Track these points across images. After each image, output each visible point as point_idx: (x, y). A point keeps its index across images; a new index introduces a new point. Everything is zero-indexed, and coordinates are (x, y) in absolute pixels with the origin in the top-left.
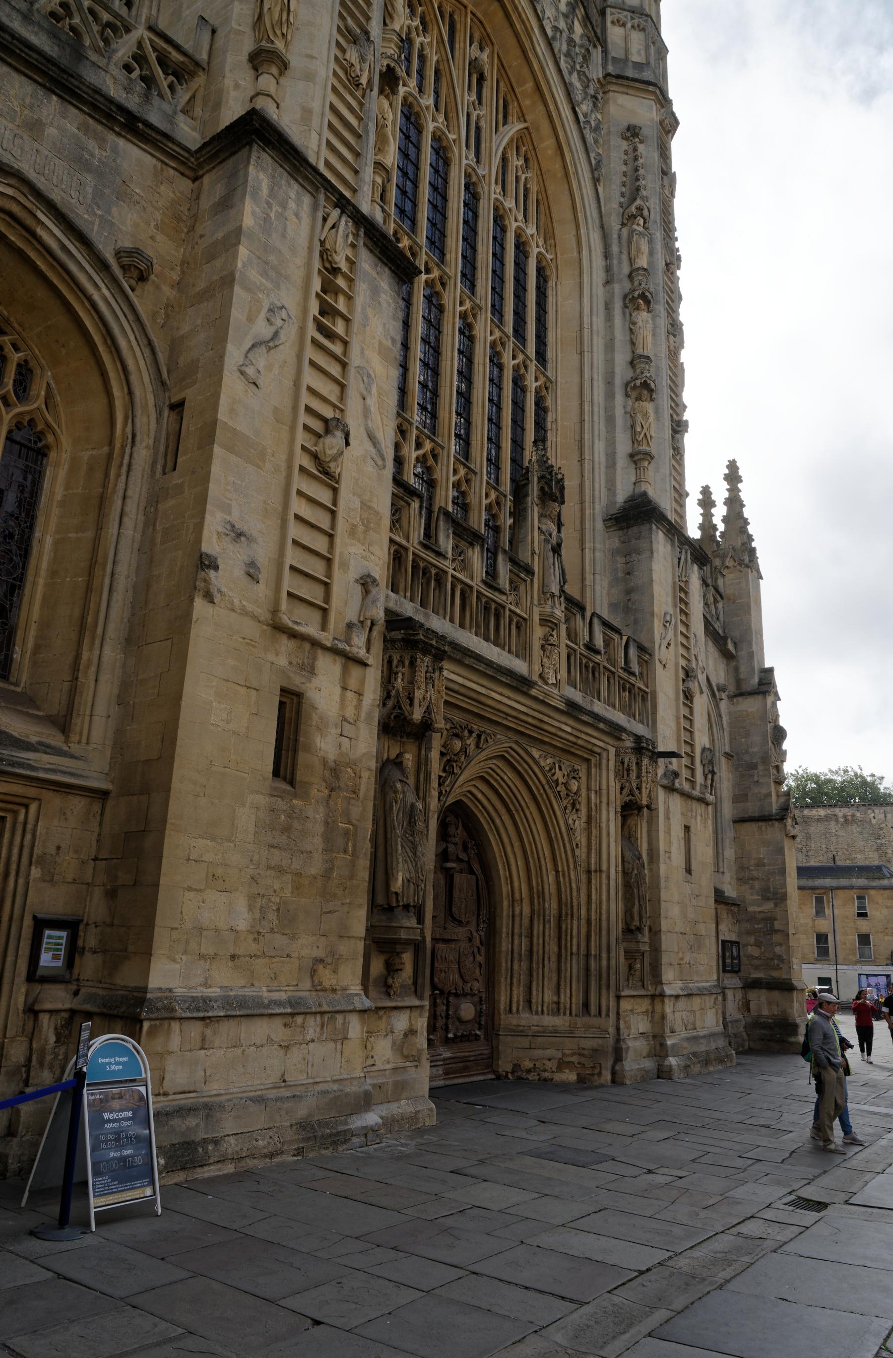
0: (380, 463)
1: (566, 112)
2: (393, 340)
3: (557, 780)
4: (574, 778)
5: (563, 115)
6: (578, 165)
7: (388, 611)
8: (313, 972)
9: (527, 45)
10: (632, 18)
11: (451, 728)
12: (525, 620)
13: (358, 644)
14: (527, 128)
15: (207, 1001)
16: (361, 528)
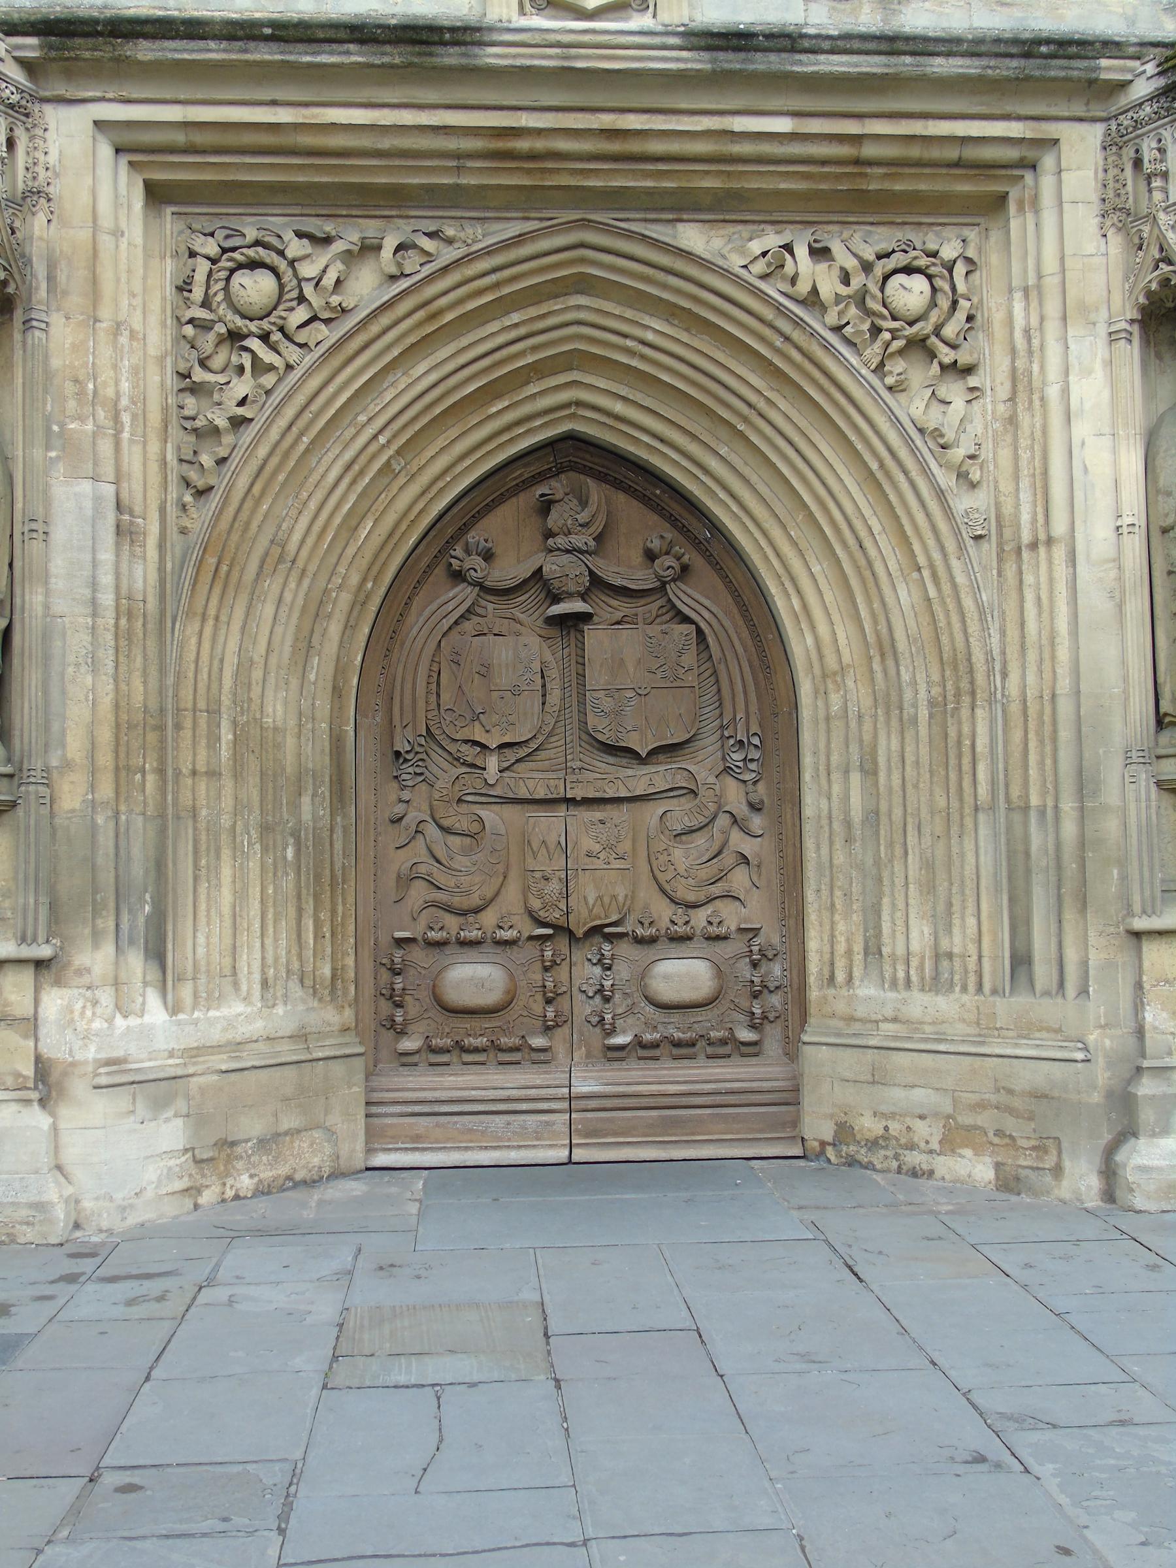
3: (815, 291)
4: (908, 270)
11: (225, 251)
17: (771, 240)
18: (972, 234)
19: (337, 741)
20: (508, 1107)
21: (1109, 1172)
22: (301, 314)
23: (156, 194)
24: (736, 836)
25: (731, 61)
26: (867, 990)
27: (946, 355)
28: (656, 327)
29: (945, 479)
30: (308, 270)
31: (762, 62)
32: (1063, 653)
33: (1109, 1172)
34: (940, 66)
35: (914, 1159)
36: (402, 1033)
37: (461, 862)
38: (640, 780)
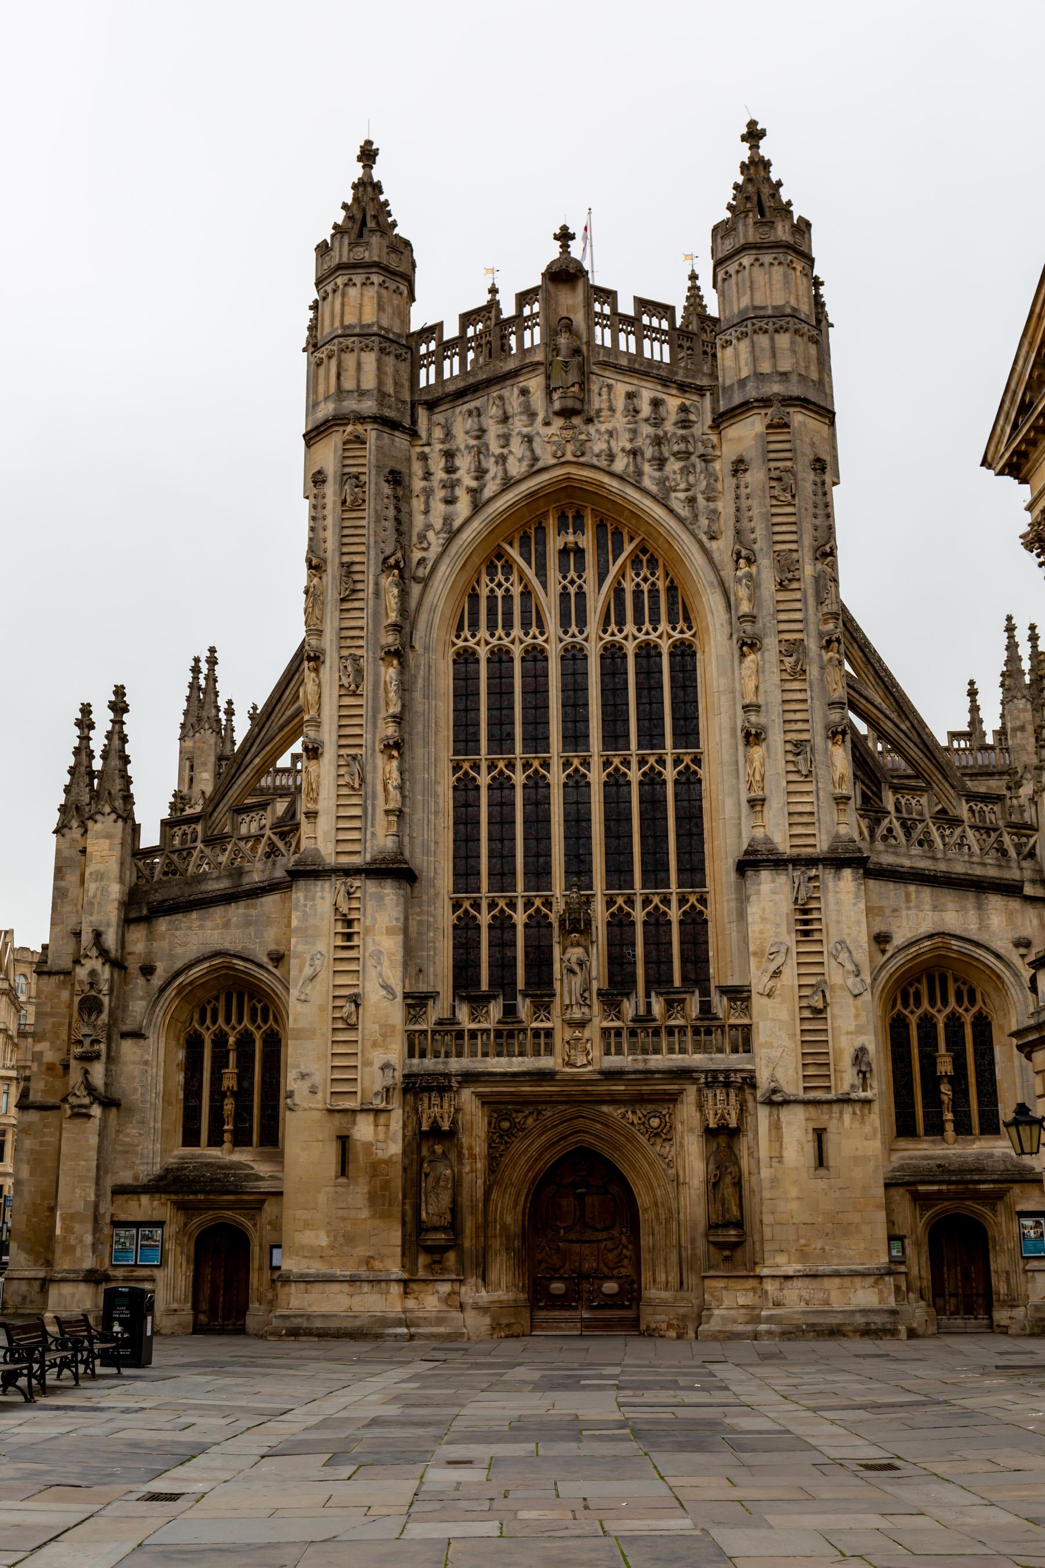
0: (391, 997)
1: (658, 512)
2: (397, 919)
4: (655, 1117)
7: (404, 1076)
12: (553, 1029)
13: (379, 1103)
14: (643, 539)
15: (307, 1275)
16: (380, 1038)
17: (623, 1110)
19: (523, 1226)
20: (566, 1320)
21: (696, 1333)
23: (483, 1103)
24: (624, 1251)
26: (653, 1291)
27: (664, 1137)
28: (599, 1126)
29: (665, 1166)
30: (517, 1120)
31: (616, 1077)
33: (696, 1333)
34: (657, 1076)
35: (662, 1333)
36: (540, 1301)
37: (554, 1257)
38: (600, 1236)
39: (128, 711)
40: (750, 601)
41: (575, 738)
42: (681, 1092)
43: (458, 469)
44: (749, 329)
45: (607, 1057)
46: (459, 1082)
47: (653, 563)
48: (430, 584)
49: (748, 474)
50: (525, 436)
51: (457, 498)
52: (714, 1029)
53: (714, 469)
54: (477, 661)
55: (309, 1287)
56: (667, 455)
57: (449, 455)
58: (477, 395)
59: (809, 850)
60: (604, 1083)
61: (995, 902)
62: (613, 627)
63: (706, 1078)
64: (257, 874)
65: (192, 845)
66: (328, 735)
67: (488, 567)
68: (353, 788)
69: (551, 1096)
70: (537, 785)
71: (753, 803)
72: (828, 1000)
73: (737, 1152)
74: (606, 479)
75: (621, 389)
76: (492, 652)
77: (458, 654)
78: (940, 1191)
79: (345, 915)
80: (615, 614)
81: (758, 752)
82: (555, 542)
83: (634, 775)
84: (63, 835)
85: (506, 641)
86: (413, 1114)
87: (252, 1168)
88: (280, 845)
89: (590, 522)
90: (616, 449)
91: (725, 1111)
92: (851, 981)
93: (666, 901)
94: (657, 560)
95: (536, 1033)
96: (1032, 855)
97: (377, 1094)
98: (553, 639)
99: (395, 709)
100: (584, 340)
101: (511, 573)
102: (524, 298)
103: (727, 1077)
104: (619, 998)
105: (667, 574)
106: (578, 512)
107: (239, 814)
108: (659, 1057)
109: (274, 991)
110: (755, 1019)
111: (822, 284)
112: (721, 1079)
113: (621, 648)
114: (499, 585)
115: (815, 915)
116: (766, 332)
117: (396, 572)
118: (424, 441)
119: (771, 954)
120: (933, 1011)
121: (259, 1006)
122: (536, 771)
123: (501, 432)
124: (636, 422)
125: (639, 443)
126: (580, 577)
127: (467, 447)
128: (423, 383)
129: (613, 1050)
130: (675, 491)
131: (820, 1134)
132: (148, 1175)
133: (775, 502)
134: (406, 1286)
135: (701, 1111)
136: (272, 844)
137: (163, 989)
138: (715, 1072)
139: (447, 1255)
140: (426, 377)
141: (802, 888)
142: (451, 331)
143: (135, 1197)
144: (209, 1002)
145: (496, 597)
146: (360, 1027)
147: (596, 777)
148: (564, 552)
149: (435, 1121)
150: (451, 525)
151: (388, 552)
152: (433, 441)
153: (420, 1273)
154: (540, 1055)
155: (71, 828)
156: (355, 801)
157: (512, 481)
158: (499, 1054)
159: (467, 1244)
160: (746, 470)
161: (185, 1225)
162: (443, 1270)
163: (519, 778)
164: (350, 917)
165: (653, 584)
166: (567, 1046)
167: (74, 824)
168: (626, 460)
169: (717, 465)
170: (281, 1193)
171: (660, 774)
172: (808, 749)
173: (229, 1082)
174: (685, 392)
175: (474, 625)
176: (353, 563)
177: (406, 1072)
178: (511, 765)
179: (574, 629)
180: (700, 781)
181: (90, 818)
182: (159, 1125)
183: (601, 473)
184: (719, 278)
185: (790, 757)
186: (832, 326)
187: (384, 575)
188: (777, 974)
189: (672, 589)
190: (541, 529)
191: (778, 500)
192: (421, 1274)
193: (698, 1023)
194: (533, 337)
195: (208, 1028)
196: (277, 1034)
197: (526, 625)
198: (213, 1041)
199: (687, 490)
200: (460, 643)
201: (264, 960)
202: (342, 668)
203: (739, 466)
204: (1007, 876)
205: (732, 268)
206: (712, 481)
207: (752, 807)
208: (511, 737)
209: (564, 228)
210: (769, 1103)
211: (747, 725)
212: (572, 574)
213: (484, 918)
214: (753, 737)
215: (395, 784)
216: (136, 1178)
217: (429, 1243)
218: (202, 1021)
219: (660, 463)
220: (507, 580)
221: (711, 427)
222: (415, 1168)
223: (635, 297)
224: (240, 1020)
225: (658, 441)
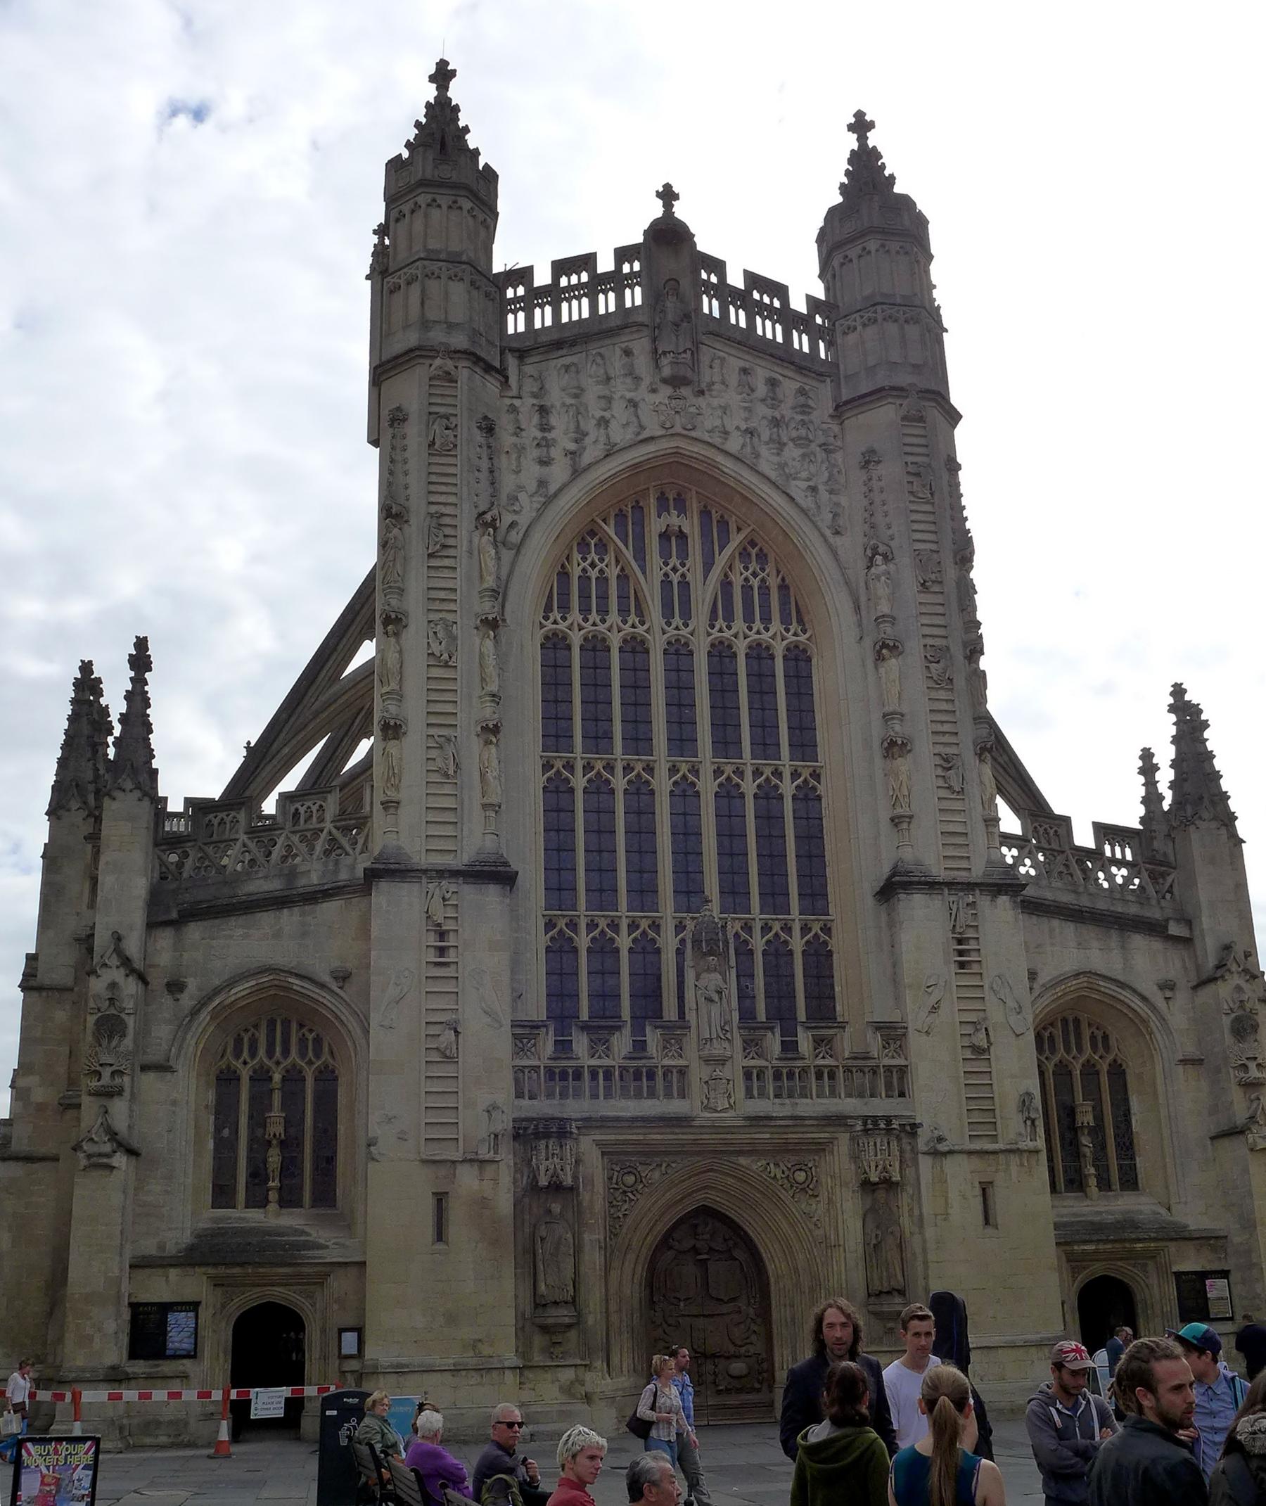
0: (496, 1025)
1: (777, 500)
4: (800, 1170)
5: (775, 505)
6: (806, 539)
7: (514, 1120)
8: (474, 1347)
9: (716, 473)
10: (862, 317)
13: (485, 1153)
18: (816, 1158)
22: (641, 1186)
23: (603, 1153)
25: (754, 1122)
28: (730, 1181)
29: (811, 1226)
30: (644, 1175)
32: (843, 1277)
34: (807, 1122)
39: (151, 670)
40: (889, 600)
41: (682, 741)
42: (831, 1141)
43: (553, 428)
44: (880, 318)
45: (750, 1102)
46: (578, 1128)
47: (762, 557)
48: (523, 551)
49: (880, 467)
50: (630, 401)
51: (553, 459)
52: (866, 1070)
53: (835, 459)
54: (569, 648)
55: (401, 1379)
56: (785, 439)
57: (543, 410)
58: (575, 350)
59: (964, 873)
60: (747, 1130)
61: (1138, 941)
62: (720, 623)
63: (865, 1124)
64: (313, 874)
65: (233, 837)
66: (414, 712)
67: (578, 544)
68: (447, 775)
69: (683, 1145)
70: (640, 791)
71: (896, 821)
72: (992, 1040)
73: (895, 1209)
74: (720, 458)
75: (735, 363)
76: (586, 639)
77: (547, 638)
78: (1096, 1252)
79: (439, 925)
80: (722, 608)
81: (903, 764)
82: (655, 525)
83: (749, 787)
84: (59, 818)
85: (602, 628)
86: (525, 1164)
87: (308, 1234)
88: (344, 842)
89: (695, 506)
90: (730, 428)
91: (887, 1162)
92: (1013, 1019)
93: (787, 929)
94: (766, 555)
95: (667, 1071)
96: (1170, 891)
97: (483, 1140)
98: (657, 630)
99: (493, 688)
100: (693, 306)
101: (606, 552)
102: (623, 254)
103: (889, 1122)
104: (762, 1032)
105: (778, 572)
106: (679, 494)
107: (291, 802)
108: (808, 1101)
109: (337, 1017)
110: (913, 1060)
111: (935, 287)
112: (882, 1126)
113: (730, 647)
114: (593, 565)
115: (972, 945)
116: (896, 321)
117: (491, 530)
118: (514, 392)
119: (928, 987)
120: (1070, 1059)
121: (311, 1037)
122: (639, 775)
123: (602, 394)
124: (751, 401)
125: (752, 424)
126: (683, 565)
127: (564, 404)
128: (511, 331)
129: (755, 1093)
130: (795, 479)
131: (986, 1188)
132: (177, 1243)
133: (913, 499)
134: (521, 1375)
135: (855, 1162)
136: (333, 840)
137: (195, 1012)
138: (875, 1119)
139: (568, 1334)
140: (515, 323)
141: (961, 913)
142: (542, 278)
143: (160, 1271)
144: (246, 1030)
145: (589, 578)
146: (460, 1060)
147: (707, 786)
148: (665, 536)
149: (555, 1174)
150: (546, 487)
151: (481, 509)
152: (523, 394)
153: (536, 1359)
154: (673, 1098)
155: (69, 810)
156: (447, 790)
157: (616, 448)
158: (625, 1094)
159: (590, 1321)
160: (879, 462)
161: (223, 1306)
162: (565, 1354)
163: (620, 782)
164: (444, 928)
165: (763, 580)
166: (705, 1087)
167: (74, 805)
168: (741, 440)
169: (839, 456)
170: (365, 1263)
171: (776, 787)
172: (960, 764)
173: (276, 1128)
174: (805, 375)
175: (565, 608)
176: (442, 515)
177: (516, 1115)
178: (610, 767)
179: (677, 621)
180: (819, 798)
181: (109, 794)
182: (190, 1180)
183: (717, 452)
184: (836, 263)
185: (940, 772)
186: (946, 331)
187: (477, 533)
188: (934, 1009)
189: (783, 587)
190: (638, 508)
191: (915, 496)
192: (538, 1359)
193: (850, 1063)
194: (634, 297)
195: (245, 1063)
196: (333, 1072)
197: (624, 611)
198: (251, 1078)
199: (809, 479)
200: (549, 625)
201: (326, 979)
202: (431, 634)
203: (869, 460)
204: (1148, 915)
205: (853, 252)
206: (836, 470)
207: (896, 825)
208: (609, 737)
209: (668, 187)
210: (935, 1153)
211: (892, 734)
212: (674, 561)
213: (583, 941)
214: (894, 748)
215: (495, 774)
216: (161, 1247)
217: (550, 1321)
218: (237, 1054)
219: (782, 445)
220: (602, 560)
221: (831, 416)
222: (527, 1230)
223: (746, 272)
224: (286, 1052)
225: (776, 423)
